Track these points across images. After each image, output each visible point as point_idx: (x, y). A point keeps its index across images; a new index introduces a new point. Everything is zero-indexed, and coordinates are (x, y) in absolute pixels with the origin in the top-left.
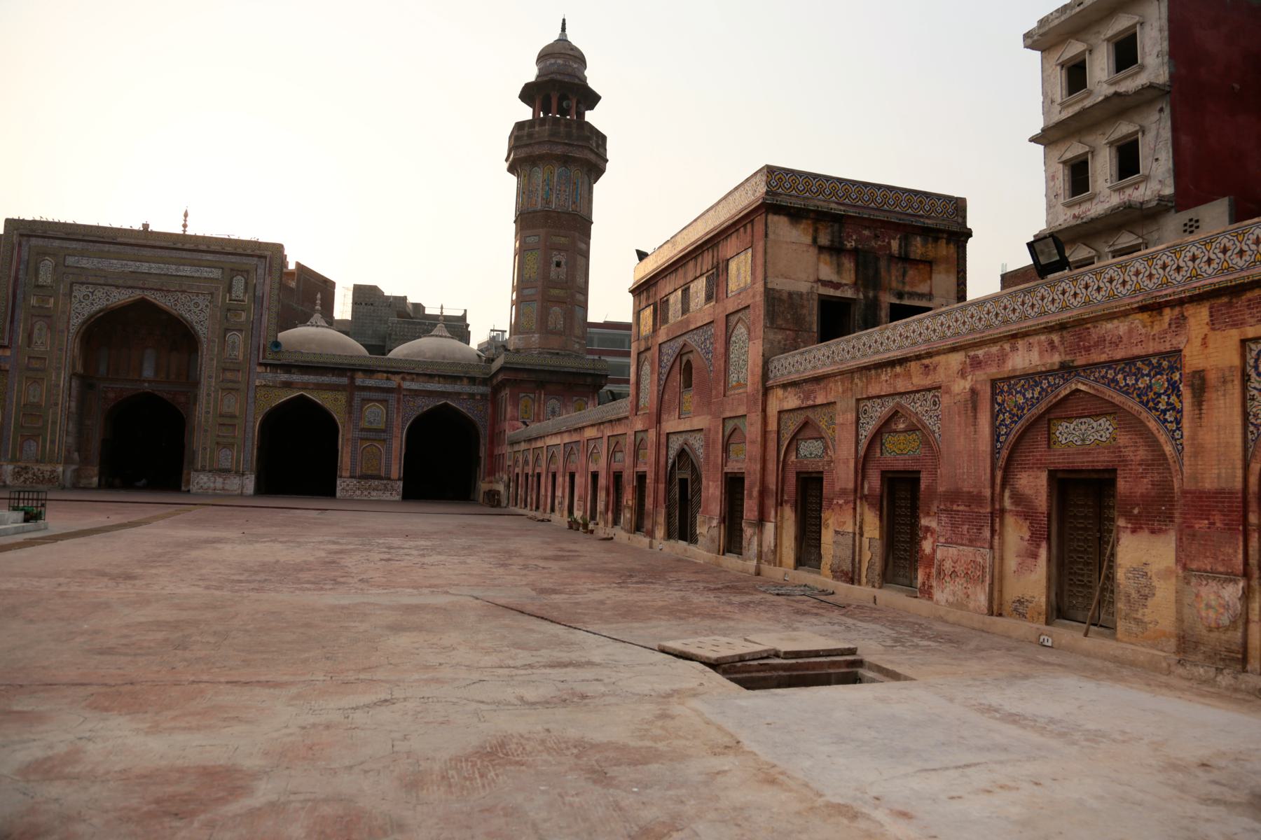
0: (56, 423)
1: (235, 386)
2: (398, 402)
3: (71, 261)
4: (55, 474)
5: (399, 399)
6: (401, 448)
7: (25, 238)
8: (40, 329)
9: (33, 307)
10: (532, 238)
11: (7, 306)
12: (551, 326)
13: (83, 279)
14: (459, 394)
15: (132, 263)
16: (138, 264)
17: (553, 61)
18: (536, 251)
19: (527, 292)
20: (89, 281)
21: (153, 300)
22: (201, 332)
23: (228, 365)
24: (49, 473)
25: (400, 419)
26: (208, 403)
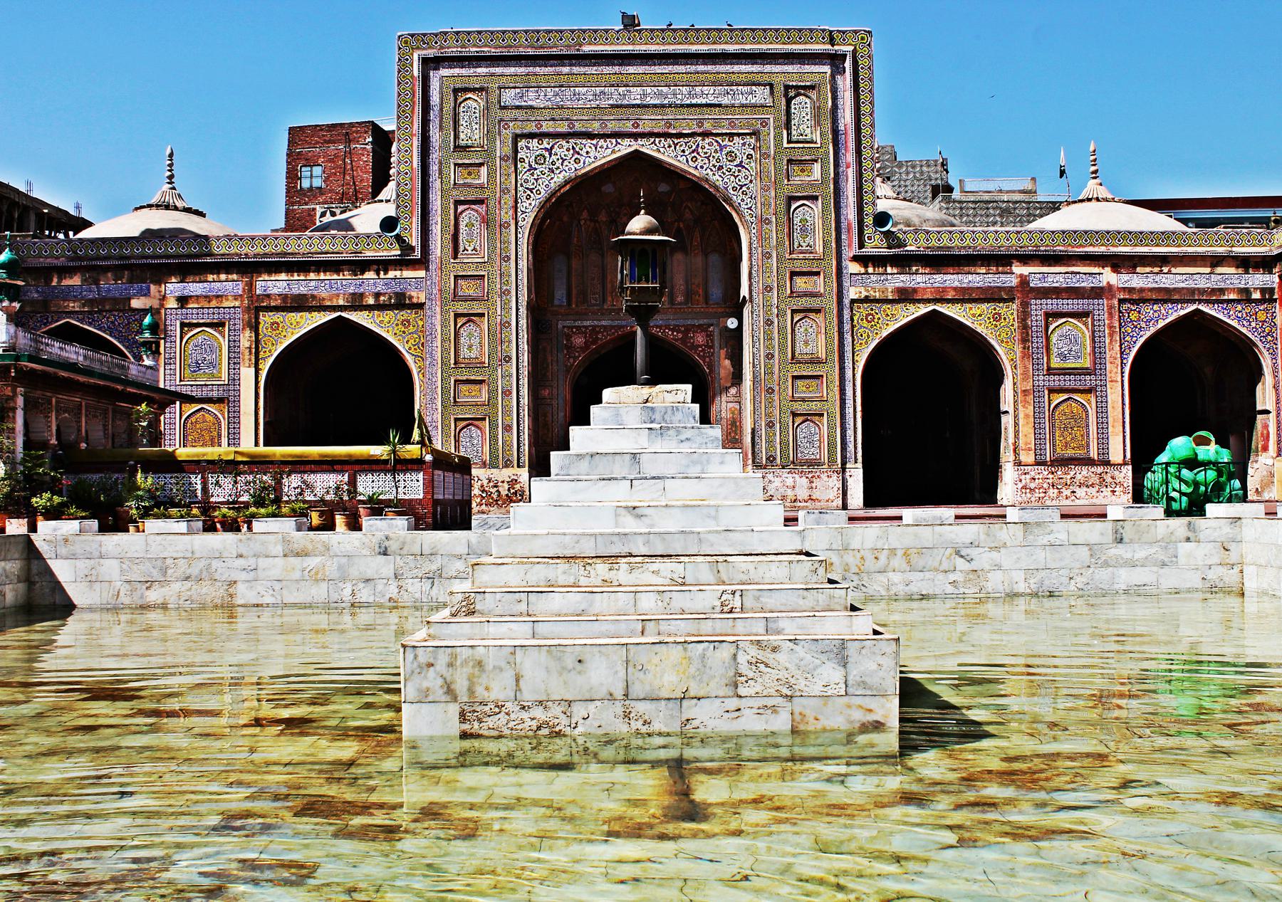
2: (1111, 315)
4: (517, 487)
6: (1123, 404)
13: (531, 128)
14: (1222, 291)
16: (621, 90)
23: (797, 263)
24: (506, 486)
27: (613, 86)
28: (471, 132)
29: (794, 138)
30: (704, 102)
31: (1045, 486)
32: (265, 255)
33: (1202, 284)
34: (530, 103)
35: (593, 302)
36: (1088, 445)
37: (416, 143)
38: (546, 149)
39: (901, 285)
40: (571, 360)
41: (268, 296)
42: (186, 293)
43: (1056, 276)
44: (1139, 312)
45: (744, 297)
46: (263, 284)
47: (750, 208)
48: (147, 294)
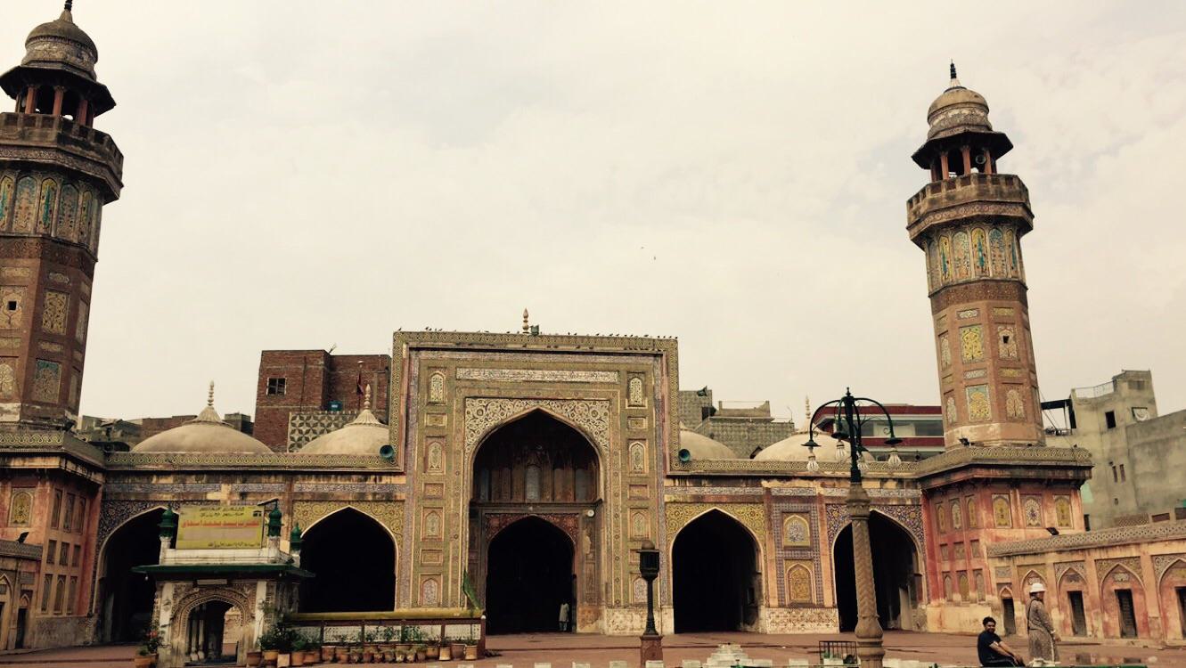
0: (458, 558)
1: (644, 504)
2: (821, 513)
3: (461, 373)
5: (822, 509)
6: (831, 569)
7: (414, 352)
8: (435, 452)
9: (427, 426)
10: (969, 313)
12: (1011, 413)
14: (888, 499)
15: (524, 371)
16: (530, 371)
17: (956, 112)
18: (976, 327)
19: (969, 375)
20: (484, 392)
23: (633, 480)
27: (525, 369)
28: (437, 393)
30: (579, 380)
32: (302, 467)
34: (475, 378)
37: (404, 399)
39: (694, 493)
41: (302, 494)
42: (246, 490)
43: (787, 489)
46: (300, 485)
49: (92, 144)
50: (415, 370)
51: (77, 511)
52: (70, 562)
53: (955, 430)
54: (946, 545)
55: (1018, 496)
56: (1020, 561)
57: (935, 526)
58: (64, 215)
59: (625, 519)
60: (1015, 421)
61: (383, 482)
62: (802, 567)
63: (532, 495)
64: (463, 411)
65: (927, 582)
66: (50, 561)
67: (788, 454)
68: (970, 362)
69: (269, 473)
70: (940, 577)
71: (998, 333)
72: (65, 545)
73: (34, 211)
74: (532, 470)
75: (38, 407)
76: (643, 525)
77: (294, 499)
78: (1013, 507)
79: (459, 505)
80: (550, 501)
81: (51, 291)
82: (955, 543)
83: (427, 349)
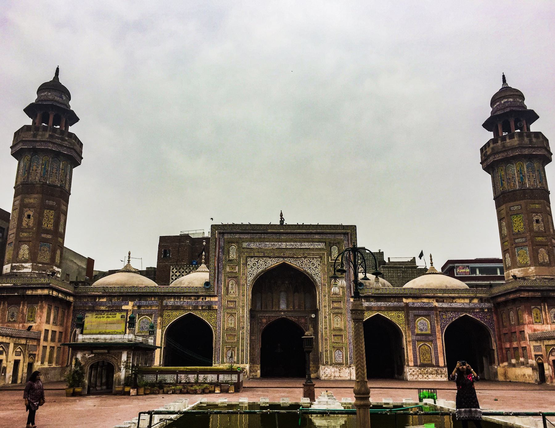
1: (340, 311)
2: (437, 317)
3: (245, 245)
5: (437, 314)
8: (232, 285)
10: (516, 208)
11: (215, 273)
13: (252, 255)
14: (474, 309)
19: (517, 241)
20: (256, 254)
21: (290, 264)
22: (317, 280)
23: (334, 298)
25: (439, 327)
26: (326, 322)
27: (277, 242)
29: (333, 259)
31: (418, 374)
32: (167, 293)
33: (467, 306)
34: (251, 247)
35: (269, 308)
36: (432, 360)
38: (256, 261)
39: (368, 305)
40: (262, 327)
41: (167, 306)
44: (446, 315)
45: (317, 309)
47: (319, 281)
48: (128, 304)
49: (67, 138)
50: (222, 244)
51: (60, 315)
52: (57, 340)
53: (510, 271)
54: (507, 333)
55: (546, 307)
56: (547, 342)
57: (501, 323)
58: (53, 173)
59: (330, 320)
60: (544, 266)
61: (206, 300)
62: (427, 345)
63: (283, 306)
64: (246, 264)
65: (497, 354)
66: (46, 339)
67: (420, 285)
68: (517, 234)
69: (152, 296)
70: (504, 351)
71: (533, 218)
72: (54, 332)
73: (39, 171)
74: (283, 294)
75: (40, 265)
76: (340, 322)
77: (163, 308)
78: (543, 313)
79: (244, 313)
80: (292, 310)
81: (47, 209)
82: (512, 333)
83: (228, 233)
